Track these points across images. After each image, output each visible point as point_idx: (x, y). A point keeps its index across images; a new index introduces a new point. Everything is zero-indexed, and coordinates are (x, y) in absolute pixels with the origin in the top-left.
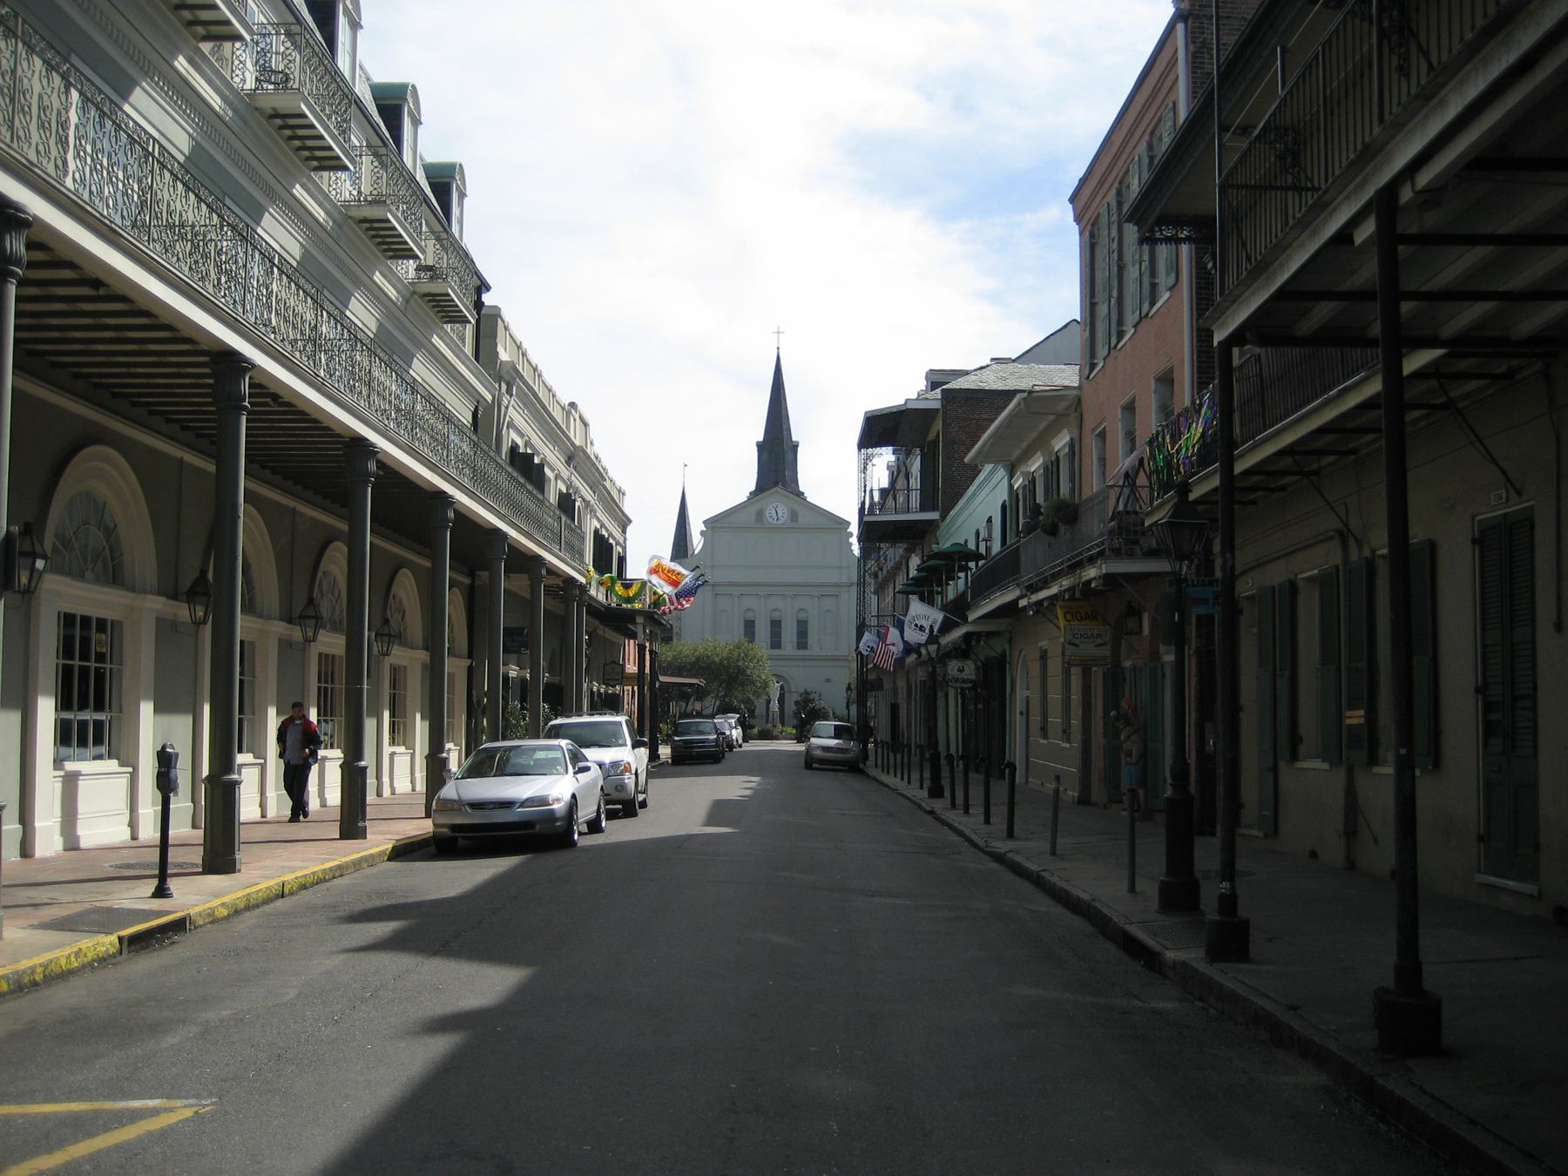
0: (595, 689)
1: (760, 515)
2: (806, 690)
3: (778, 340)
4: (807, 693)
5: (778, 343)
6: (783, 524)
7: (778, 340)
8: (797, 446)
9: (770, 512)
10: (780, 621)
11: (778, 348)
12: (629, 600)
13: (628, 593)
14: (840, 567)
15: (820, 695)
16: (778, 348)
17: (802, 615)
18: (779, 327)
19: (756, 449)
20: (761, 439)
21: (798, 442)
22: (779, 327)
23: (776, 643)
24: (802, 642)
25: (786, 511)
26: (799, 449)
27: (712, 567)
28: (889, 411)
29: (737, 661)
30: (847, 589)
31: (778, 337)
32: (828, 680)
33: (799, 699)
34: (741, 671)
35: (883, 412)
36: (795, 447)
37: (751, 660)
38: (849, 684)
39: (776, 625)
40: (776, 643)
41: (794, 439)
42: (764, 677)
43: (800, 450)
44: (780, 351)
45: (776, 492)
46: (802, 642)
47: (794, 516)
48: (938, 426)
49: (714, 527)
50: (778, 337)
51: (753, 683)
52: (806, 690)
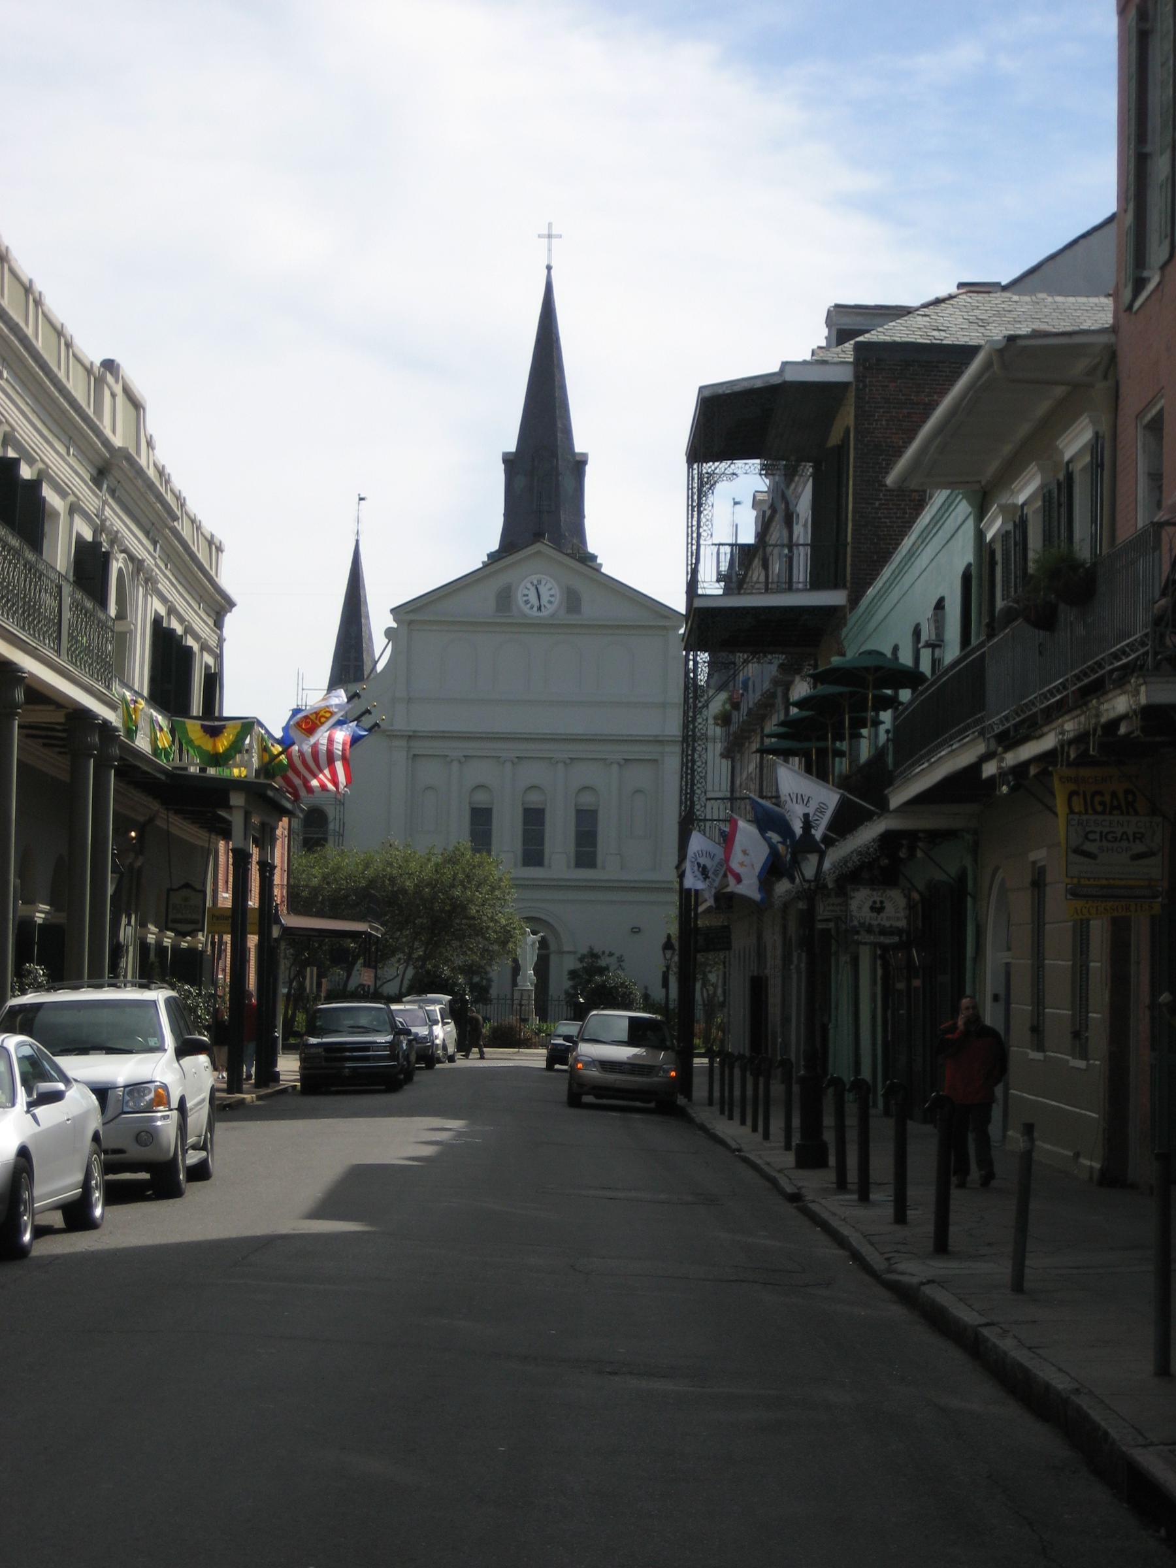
0: (151, 938)
1: (505, 598)
2: (591, 949)
3: (550, 250)
4: (594, 955)
6: (552, 616)
7: (550, 250)
9: (524, 594)
11: (549, 268)
12: (218, 760)
13: (215, 745)
15: (620, 959)
16: (549, 268)
17: (587, 800)
19: (502, 467)
20: (511, 445)
21: (585, 455)
23: (533, 855)
25: (556, 591)
27: (409, 700)
28: (747, 385)
29: (453, 886)
32: (636, 931)
33: (579, 966)
34: (458, 908)
35: (737, 388)
36: (580, 464)
37: (479, 885)
38: (669, 937)
39: (534, 818)
40: (533, 855)
41: (578, 448)
42: (503, 922)
43: (589, 469)
44: (553, 271)
45: (539, 553)
47: (573, 601)
48: (847, 417)
49: (411, 623)
51: (480, 932)
52: (591, 949)
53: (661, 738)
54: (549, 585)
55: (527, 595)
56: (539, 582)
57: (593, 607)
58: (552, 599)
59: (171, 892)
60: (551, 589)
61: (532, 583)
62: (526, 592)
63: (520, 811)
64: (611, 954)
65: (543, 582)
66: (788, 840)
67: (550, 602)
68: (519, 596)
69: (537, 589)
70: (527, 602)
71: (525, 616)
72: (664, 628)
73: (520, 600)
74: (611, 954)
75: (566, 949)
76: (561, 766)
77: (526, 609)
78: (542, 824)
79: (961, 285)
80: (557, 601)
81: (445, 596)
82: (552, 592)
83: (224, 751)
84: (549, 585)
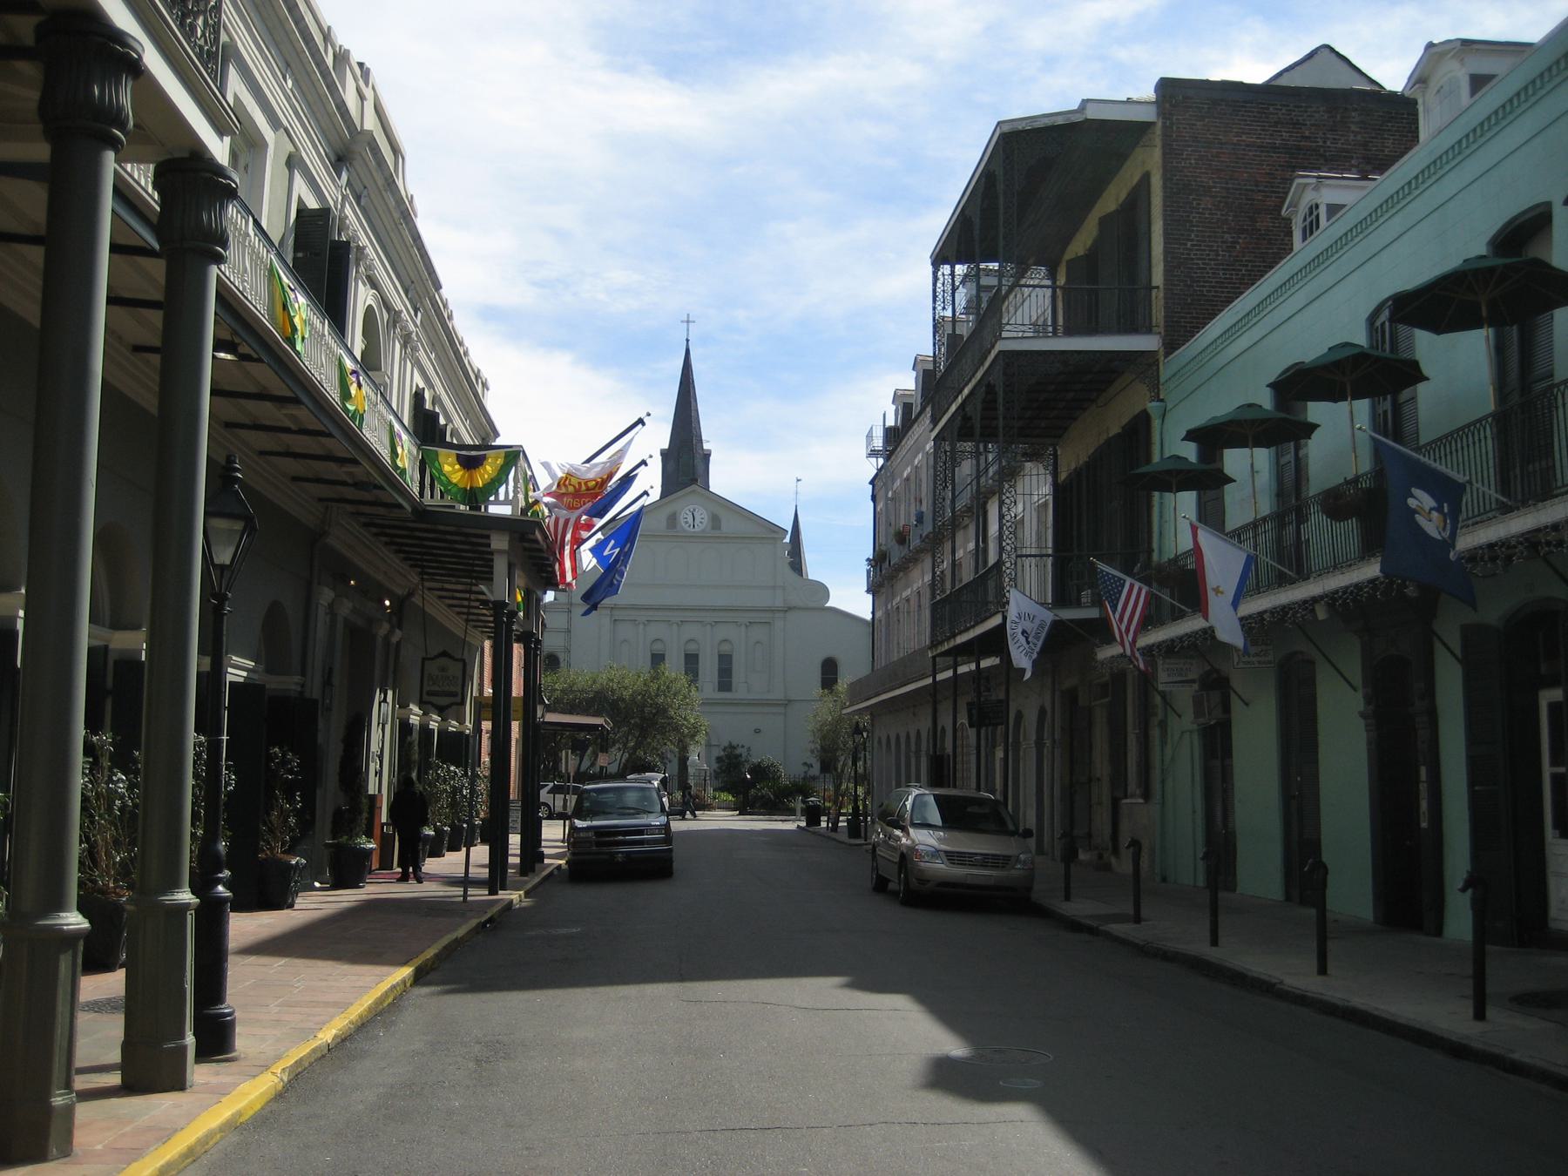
0: (415, 720)
1: (672, 520)
2: (730, 743)
3: (688, 330)
4: (732, 747)
5: (688, 334)
6: (703, 531)
7: (688, 330)
8: (709, 455)
9: (685, 517)
11: (688, 340)
12: (476, 497)
13: (471, 478)
14: (774, 588)
15: (749, 749)
16: (688, 340)
17: (725, 648)
18: (688, 315)
19: (660, 458)
20: (666, 446)
21: (710, 451)
22: (688, 315)
24: (725, 683)
25: (705, 516)
26: (711, 458)
28: (1048, 122)
29: (657, 695)
30: (782, 615)
31: (688, 326)
32: (757, 731)
33: (722, 753)
34: (662, 711)
35: (1038, 125)
36: (706, 456)
37: (675, 695)
41: (705, 447)
42: (693, 721)
45: (694, 491)
46: (725, 683)
47: (715, 521)
48: (1150, 160)
50: (688, 326)
51: (677, 729)
52: (730, 743)
56: (694, 510)
57: (729, 525)
59: (426, 662)
62: (686, 516)
64: (743, 747)
66: (1445, 505)
67: (701, 522)
68: (682, 517)
70: (687, 523)
71: (685, 531)
72: (774, 538)
74: (743, 747)
75: (713, 743)
76: (709, 627)
77: (686, 526)
78: (697, 663)
79: (913, 369)
80: (705, 521)
82: (702, 516)
83: (484, 485)
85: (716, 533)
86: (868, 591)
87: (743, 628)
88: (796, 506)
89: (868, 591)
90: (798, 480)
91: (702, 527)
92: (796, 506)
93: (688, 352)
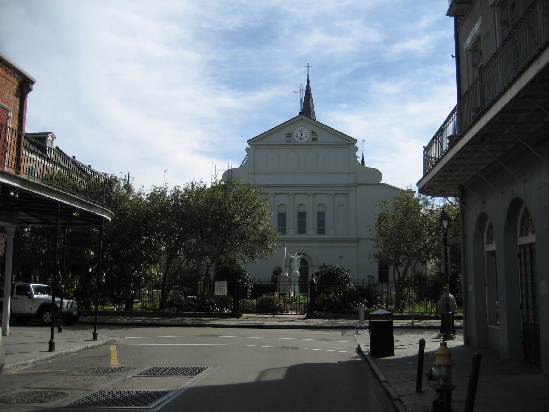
1: (289, 136)
2: (324, 264)
3: (308, 70)
6: (307, 141)
7: (308, 70)
9: (296, 134)
10: (305, 214)
14: (349, 173)
17: (321, 209)
23: (302, 229)
24: (321, 230)
25: (308, 133)
27: (255, 174)
30: (354, 189)
32: (341, 257)
33: (319, 271)
39: (302, 216)
40: (302, 229)
46: (321, 230)
47: (314, 136)
49: (255, 145)
52: (324, 264)
53: (348, 185)
54: (305, 131)
55: (297, 135)
56: (302, 130)
57: (322, 138)
58: (307, 136)
60: (306, 132)
61: (299, 130)
62: (297, 133)
63: (296, 215)
65: (303, 130)
67: (306, 137)
69: (301, 132)
70: (297, 137)
72: (349, 145)
73: (295, 136)
75: (314, 265)
77: (297, 140)
78: (305, 218)
80: (308, 136)
81: (266, 136)
82: (306, 133)
84: (305, 131)
85: (314, 143)
86: (449, 14)
87: (331, 196)
88: (363, 153)
89: (449, 14)
90: (363, 141)
91: (306, 139)
92: (363, 153)
93: (308, 81)
